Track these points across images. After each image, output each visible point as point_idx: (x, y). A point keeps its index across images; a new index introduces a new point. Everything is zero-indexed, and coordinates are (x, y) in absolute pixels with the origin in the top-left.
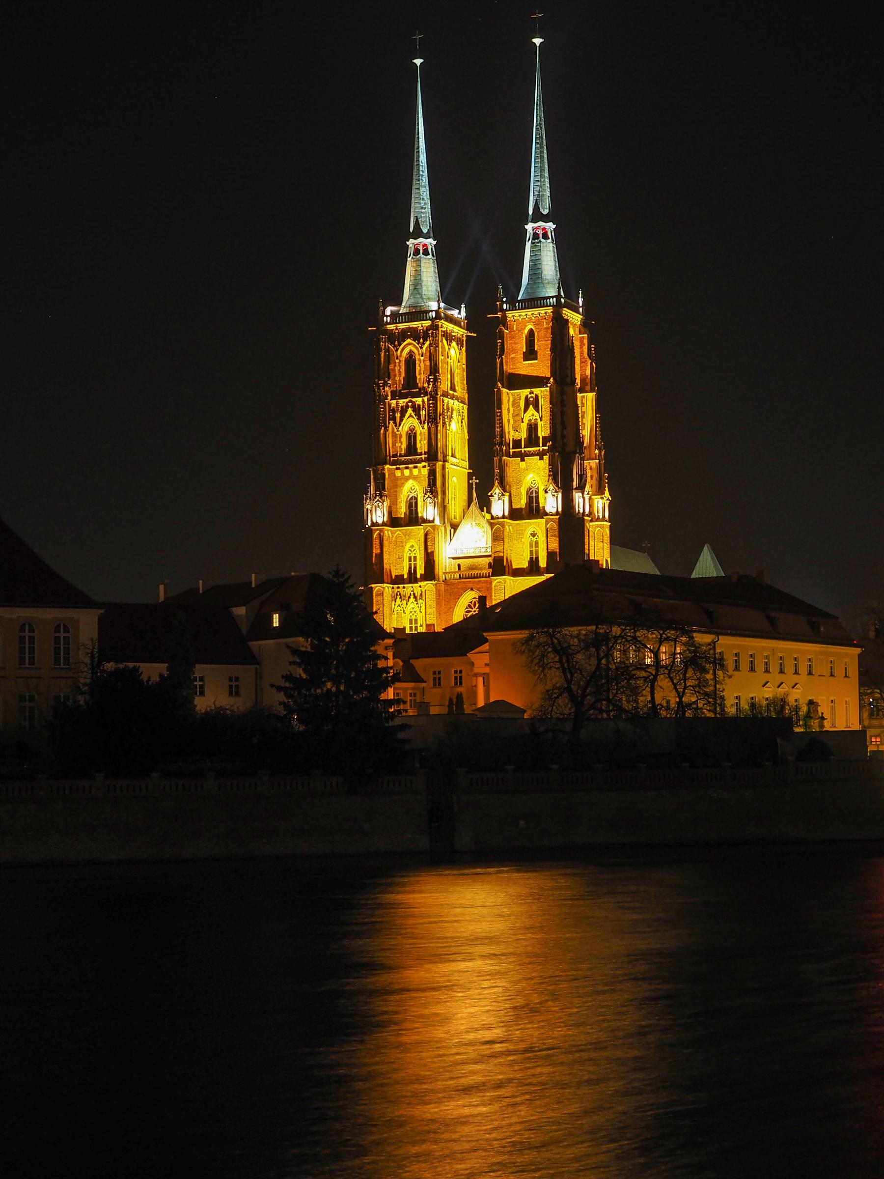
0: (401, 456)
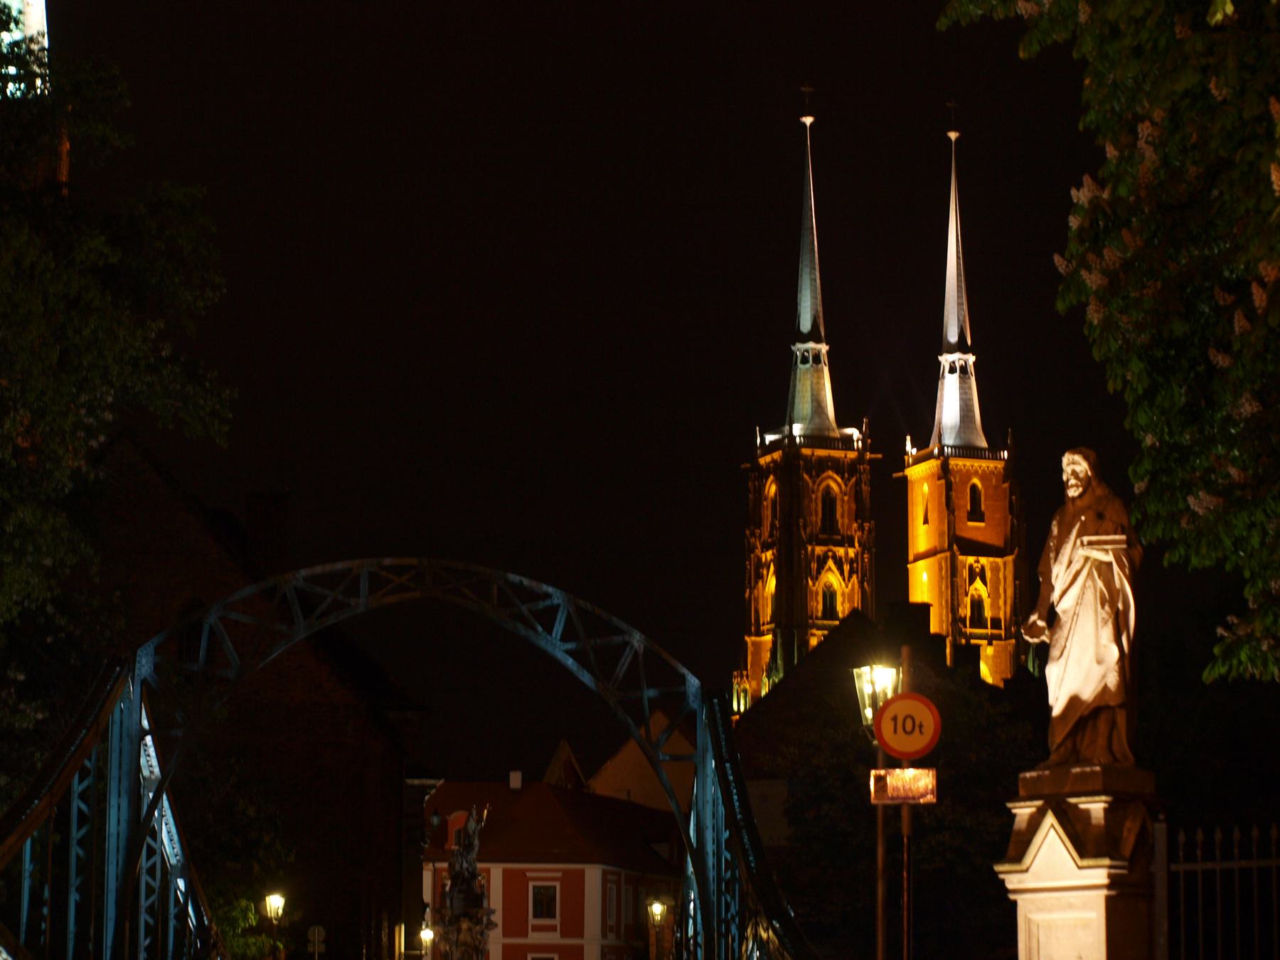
0: (817, 618)
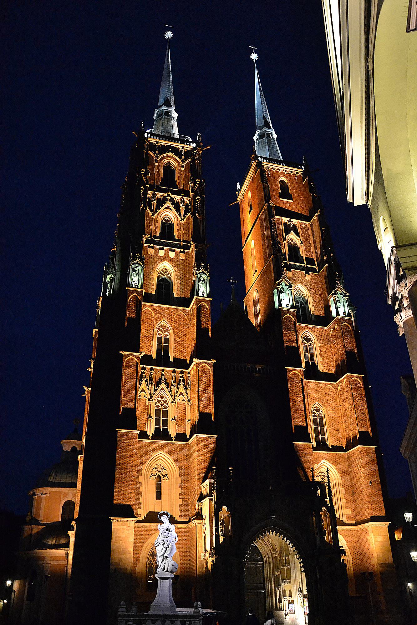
0: (155, 237)
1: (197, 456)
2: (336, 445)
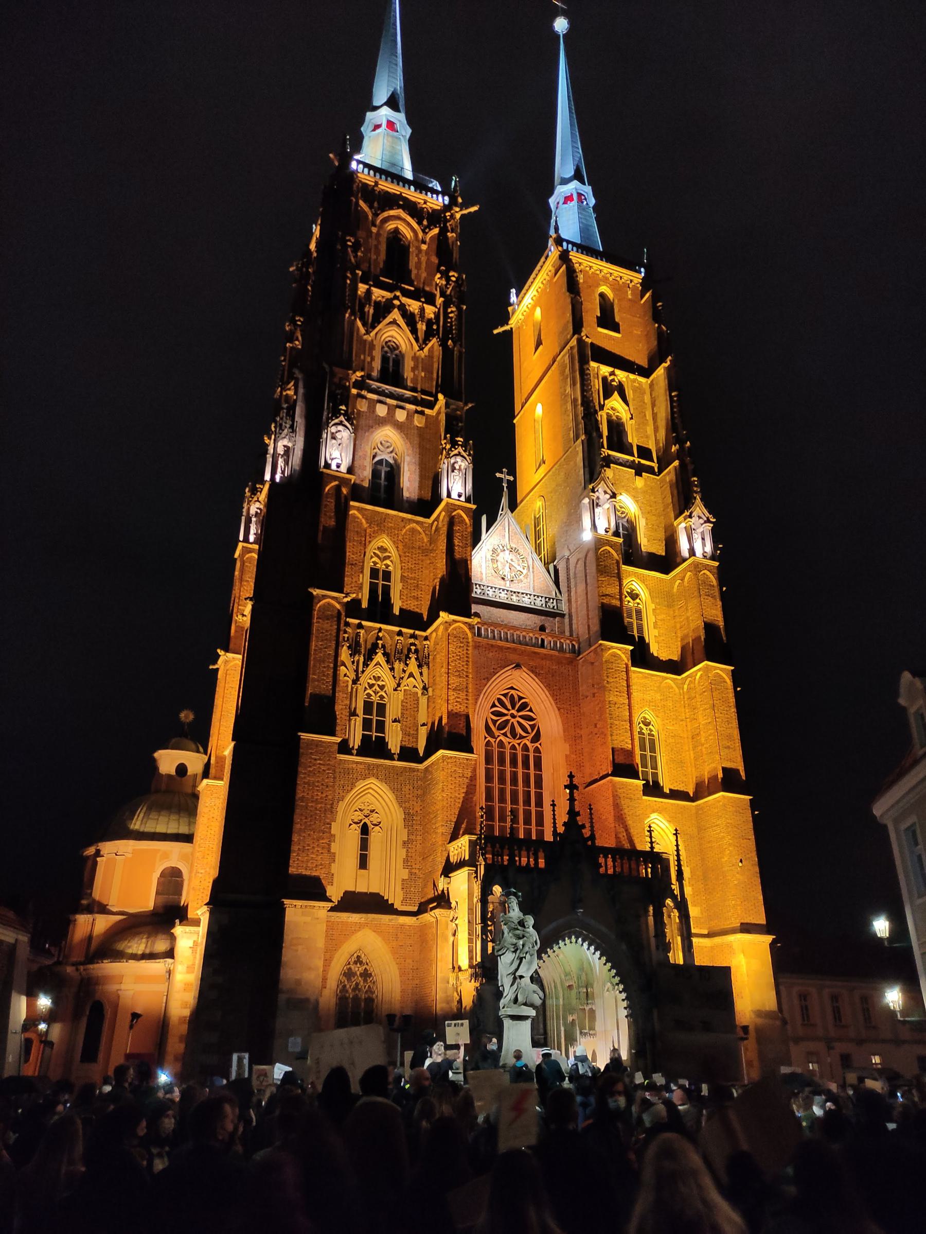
1: (443, 791)
2: (676, 789)
